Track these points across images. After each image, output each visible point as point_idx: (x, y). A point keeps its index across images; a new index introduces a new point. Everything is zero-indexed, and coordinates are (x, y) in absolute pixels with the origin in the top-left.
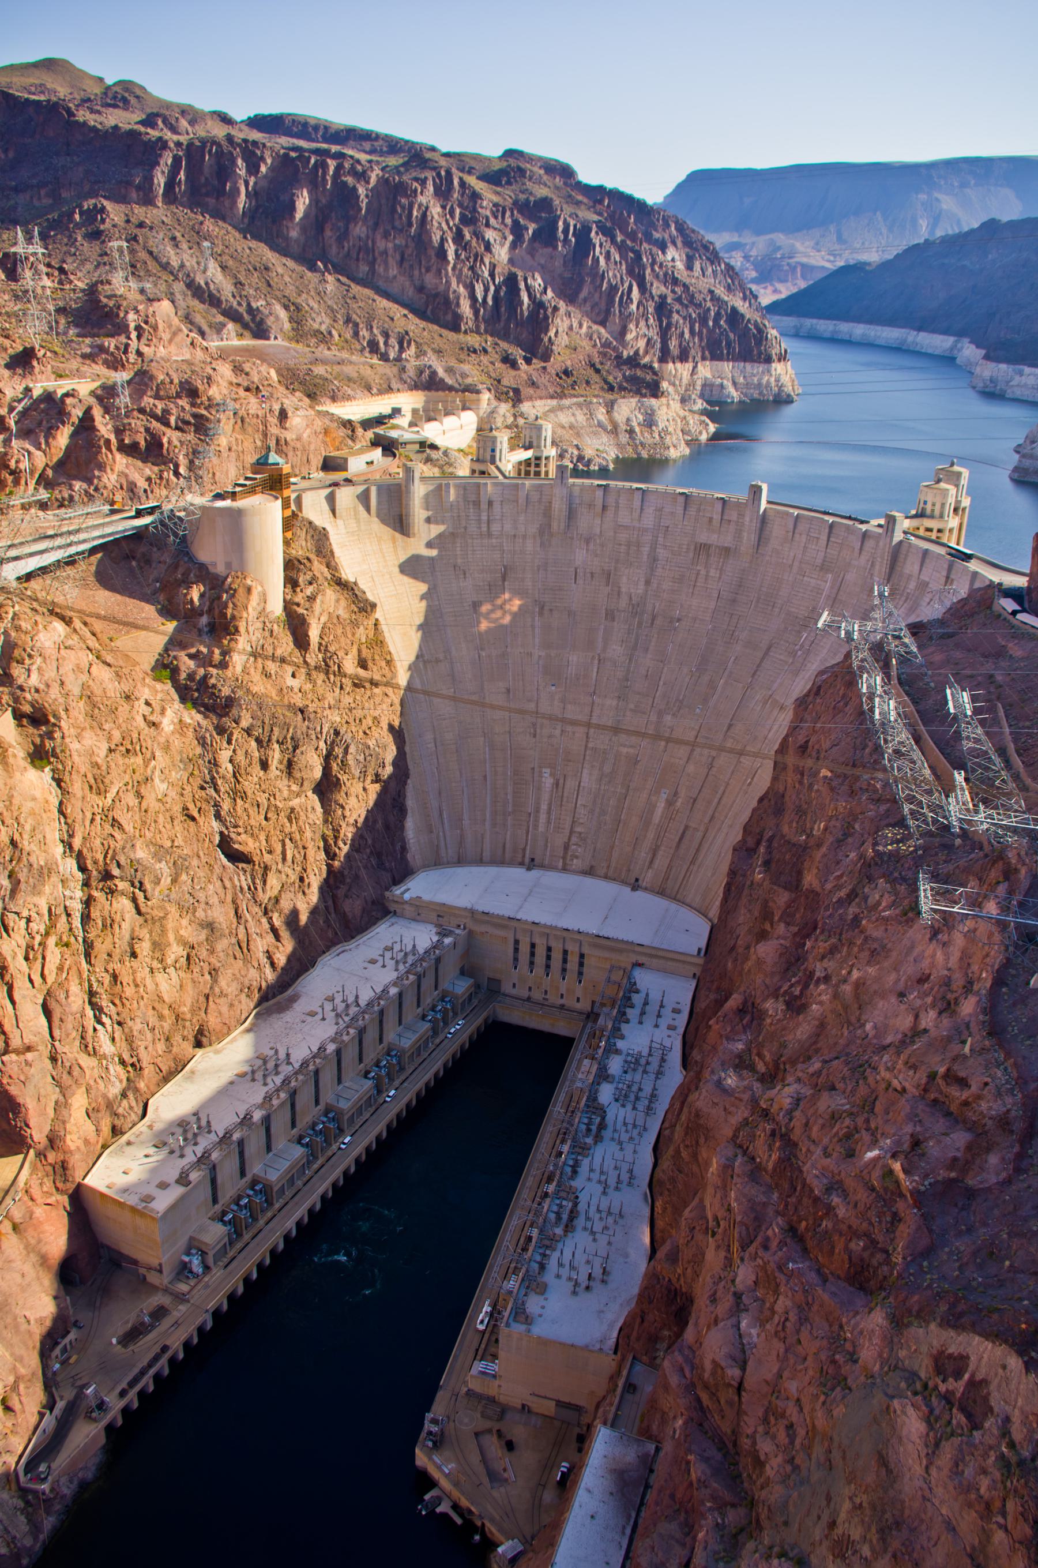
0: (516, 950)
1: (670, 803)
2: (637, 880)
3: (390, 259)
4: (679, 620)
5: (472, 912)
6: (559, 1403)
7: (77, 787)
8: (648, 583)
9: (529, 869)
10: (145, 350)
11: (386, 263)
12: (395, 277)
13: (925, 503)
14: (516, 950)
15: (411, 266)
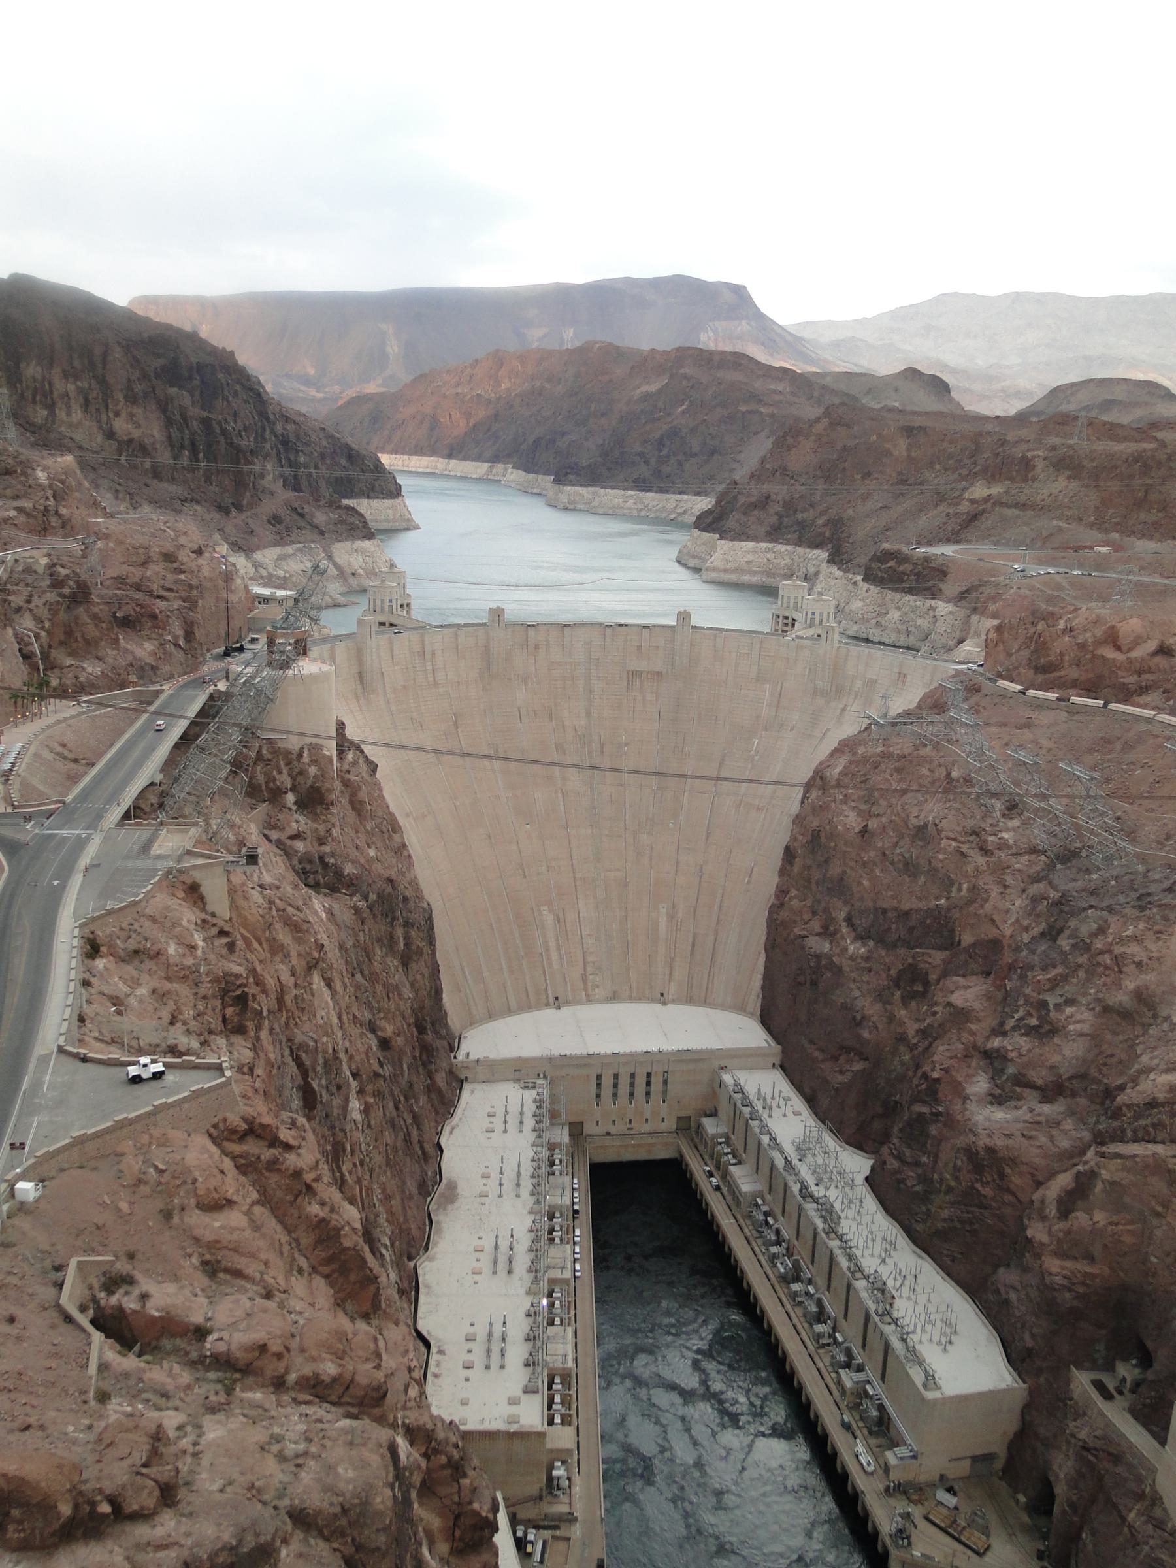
0: (599, 1085)
1: (671, 916)
2: (662, 995)
3: (73, 401)
4: (626, 745)
5: (551, 1059)
6: (975, 1459)
7: (338, 985)
8: (588, 714)
9: (558, 1008)
10: (63, 511)
11: (68, 407)
12: (80, 423)
13: (813, 614)
14: (599, 1085)
15: (98, 410)
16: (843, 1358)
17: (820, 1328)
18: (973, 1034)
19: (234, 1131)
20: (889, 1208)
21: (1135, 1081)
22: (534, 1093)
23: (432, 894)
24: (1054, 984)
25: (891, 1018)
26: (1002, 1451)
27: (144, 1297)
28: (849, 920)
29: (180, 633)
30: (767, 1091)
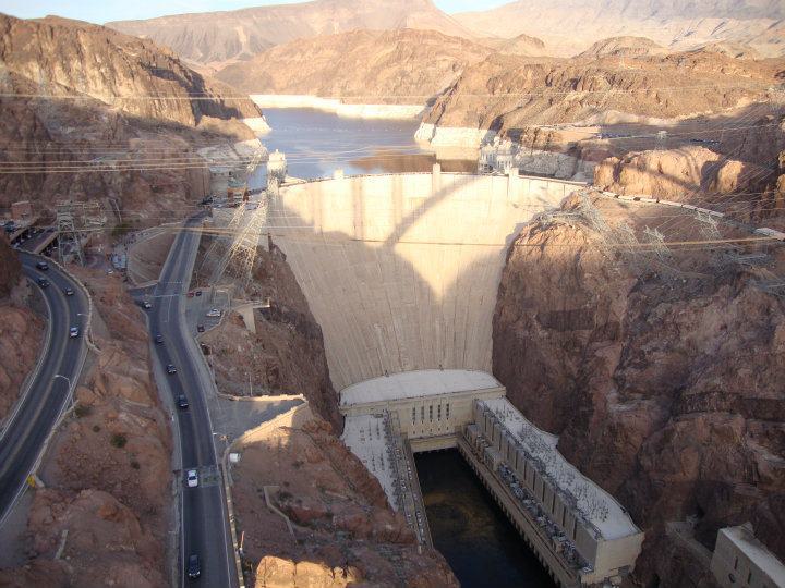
1: (441, 325)
11: (96, 84)
16: (553, 531)
17: (540, 519)
18: (607, 369)
19: (313, 428)
20: (569, 461)
21: (691, 386)
22: (381, 420)
23: (319, 321)
24: (647, 341)
25: (564, 367)
26: (633, 565)
27: (300, 502)
28: (538, 318)
29: (183, 194)
30: (501, 409)
